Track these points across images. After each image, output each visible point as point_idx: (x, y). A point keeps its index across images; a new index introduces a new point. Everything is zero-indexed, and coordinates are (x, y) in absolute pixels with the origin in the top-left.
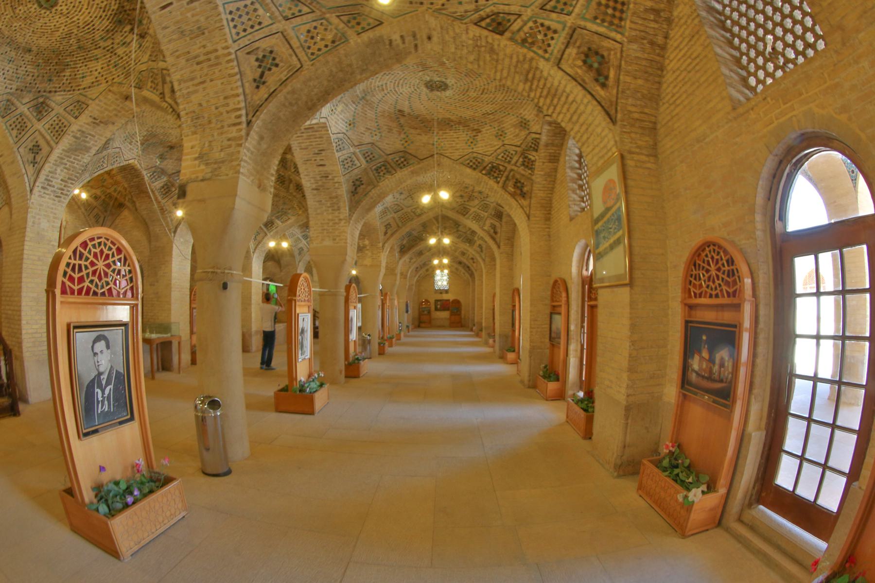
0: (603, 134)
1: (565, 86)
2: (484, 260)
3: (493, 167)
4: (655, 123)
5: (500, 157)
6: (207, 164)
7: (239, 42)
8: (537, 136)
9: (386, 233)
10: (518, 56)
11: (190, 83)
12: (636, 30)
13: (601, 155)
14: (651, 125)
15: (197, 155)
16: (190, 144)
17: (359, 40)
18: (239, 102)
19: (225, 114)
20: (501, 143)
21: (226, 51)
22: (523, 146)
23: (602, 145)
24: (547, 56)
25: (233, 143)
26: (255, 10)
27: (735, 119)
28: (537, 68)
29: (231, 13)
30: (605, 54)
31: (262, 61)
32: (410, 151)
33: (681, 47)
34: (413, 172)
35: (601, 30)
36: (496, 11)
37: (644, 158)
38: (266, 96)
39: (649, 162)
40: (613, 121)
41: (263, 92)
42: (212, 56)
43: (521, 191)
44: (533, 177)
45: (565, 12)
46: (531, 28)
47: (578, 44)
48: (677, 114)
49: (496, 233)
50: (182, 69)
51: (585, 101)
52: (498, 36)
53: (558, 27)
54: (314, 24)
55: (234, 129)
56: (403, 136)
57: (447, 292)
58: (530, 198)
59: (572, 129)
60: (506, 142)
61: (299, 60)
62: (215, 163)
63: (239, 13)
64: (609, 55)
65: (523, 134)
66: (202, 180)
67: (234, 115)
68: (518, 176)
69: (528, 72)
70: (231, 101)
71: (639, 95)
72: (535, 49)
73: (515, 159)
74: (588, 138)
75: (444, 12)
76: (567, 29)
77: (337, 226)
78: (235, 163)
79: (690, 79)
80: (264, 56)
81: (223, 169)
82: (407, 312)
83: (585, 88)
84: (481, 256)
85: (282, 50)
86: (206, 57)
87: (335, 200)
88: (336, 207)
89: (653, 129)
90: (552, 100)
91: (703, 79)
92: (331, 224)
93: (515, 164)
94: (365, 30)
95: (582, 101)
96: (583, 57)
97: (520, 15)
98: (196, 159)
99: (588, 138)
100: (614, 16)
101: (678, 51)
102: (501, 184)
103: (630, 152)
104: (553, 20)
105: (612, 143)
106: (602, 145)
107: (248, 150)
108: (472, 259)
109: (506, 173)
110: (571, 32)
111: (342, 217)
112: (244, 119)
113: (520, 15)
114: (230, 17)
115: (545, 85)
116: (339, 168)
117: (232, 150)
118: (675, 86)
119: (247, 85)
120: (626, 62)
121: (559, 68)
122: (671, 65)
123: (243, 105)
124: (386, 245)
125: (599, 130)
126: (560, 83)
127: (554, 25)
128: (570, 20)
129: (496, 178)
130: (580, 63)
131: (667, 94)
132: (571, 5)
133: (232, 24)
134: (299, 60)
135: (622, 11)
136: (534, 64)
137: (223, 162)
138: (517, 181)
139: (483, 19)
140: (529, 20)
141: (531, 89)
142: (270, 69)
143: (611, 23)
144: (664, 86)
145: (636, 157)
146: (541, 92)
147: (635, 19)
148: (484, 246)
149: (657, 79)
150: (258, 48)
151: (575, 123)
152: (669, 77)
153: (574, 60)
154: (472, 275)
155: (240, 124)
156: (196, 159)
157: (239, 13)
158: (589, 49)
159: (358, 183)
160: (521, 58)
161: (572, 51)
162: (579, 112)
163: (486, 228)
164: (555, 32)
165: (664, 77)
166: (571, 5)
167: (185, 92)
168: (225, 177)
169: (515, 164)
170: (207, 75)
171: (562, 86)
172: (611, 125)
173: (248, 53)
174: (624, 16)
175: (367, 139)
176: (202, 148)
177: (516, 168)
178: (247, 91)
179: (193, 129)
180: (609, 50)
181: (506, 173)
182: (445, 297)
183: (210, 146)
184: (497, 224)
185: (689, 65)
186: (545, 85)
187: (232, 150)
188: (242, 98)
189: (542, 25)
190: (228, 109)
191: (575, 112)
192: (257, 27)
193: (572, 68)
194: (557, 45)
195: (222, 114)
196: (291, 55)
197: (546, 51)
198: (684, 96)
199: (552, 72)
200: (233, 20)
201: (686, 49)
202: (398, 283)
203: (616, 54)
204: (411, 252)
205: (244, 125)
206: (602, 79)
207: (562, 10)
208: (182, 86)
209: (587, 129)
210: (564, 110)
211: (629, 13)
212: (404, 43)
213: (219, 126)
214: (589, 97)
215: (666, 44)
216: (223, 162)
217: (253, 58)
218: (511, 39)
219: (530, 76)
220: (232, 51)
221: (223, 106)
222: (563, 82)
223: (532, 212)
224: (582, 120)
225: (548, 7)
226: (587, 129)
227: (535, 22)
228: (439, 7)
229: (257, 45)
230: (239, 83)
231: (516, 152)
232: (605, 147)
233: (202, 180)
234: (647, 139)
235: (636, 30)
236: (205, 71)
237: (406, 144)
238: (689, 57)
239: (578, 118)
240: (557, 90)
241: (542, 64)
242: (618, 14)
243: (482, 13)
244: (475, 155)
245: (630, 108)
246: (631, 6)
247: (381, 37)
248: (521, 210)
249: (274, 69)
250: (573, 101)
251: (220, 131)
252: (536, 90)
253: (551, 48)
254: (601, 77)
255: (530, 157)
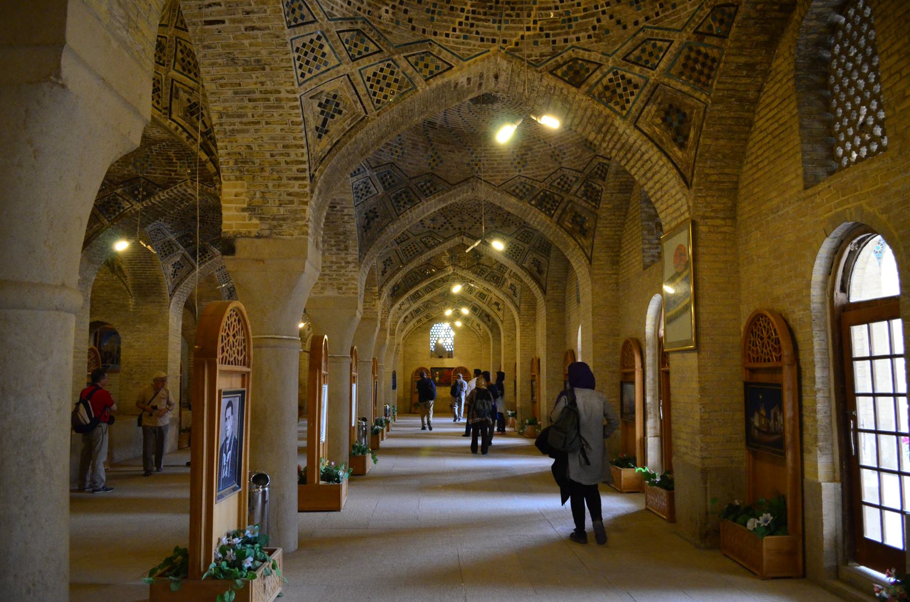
0: (678, 197)
1: (641, 146)
2: (517, 307)
3: (546, 195)
4: (737, 183)
5: (555, 184)
6: (261, 219)
7: (305, 85)
8: (605, 161)
9: (384, 272)
10: (593, 111)
11: (236, 120)
12: (723, 90)
13: (674, 215)
14: (731, 185)
15: (245, 206)
16: (234, 191)
17: (428, 88)
18: (303, 155)
19: (283, 165)
20: (557, 166)
21: (291, 96)
22: (587, 172)
23: (676, 207)
24: (624, 112)
25: (296, 199)
26: (321, 46)
27: (804, 199)
28: (612, 125)
29: (297, 50)
30: (688, 112)
31: (325, 107)
32: (437, 173)
33: (773, 106)
34: (439, 201)
35: (686, 89)
36: (574, 56)
37: (720, 222)
38: (329, 147)
39: (725, 225)
40: (688, 185)
41: (325, 144)
42: (272, 97)
43: (582, 227)
44: (598, 212)
45: (649, 65)
46: (611, 80)
47: (659, 100)
48: (757, 178)
49: (540, 272)
50: (225, 101)
51: (661, 163)
52: (574, 89)
53: (641, 82)
54: (381, 65)
55: (297, 183)
56: (430, 153)
57: (450, 355)
58: (594, 237)
59: (645, 184)
60: (564, 165)
61: (364, 108)
62: (274, 219)
63: (305, 50)
64: (692, 113)
65: (587, 155)
66: (257, 237)
67: (295, 168)
68: (578, 209)
69: (602, 126)
70: (292, 152)
71: (720, 156)
72: (612, 104)
73: (575, 188)
74: (662, 196)
75: (517, 54)
76: (648, 85)
77: (343, 271)
78: (300, 223)
79: (773, 145)
80: (327, 101)
81: (285, 227)
82: (394, 387)
83: (661, 150)
84: (513, 302)
85: (347, 95)
86: (263, 96)
87: (342, 237)
88: (343, 246)
89: (734, 190)
90: (626, 154)
91: (784, 150)
92: (334, 268)
93: (575, 194)
94: (433, 75)
95: (657, 162)
96: (662, 114)
97: (600, 65)
98: (244, 210)
99: (662, 196)
100: (701, 73)
101: (767, 110)
102: (555, 219)
103: (704, 217)
104: (634, 74)
105: (685, 208)
106: (676, 207)
107: (311, 206)
108: (497, 304)
109: (563, 205)
110: (652, 89)
111: (350, 259)
112: (307, 174)
113: (600, 65)
114: (296, 55)
115: (619, 139)
116: (350, 197)
117: (294, 206)
118: (760, 148)
119: (310, 134)
120: (708, 124)
121: (636, 127)
122: (760, 123)
123: (305, 158)
124: (384, 289)
125: (673, 192)
126: (635, 142)
127: (635, 79)
128: (653, 76)
129: (549, 210)
130: (658, 121)
131: (752, 154)
132: (657, 58)
133: (298, 64)
134: (364, 108)
135: (711, 69)
136: (610, 121)
137: (284, 219)
138: (577, 215)
139: (559, 66)
140: (608, 72)
141: (603, 140)
142: (333, 117)
143: (698, 81)
144: (751, 144)
145: (710, 222)
146: (615, 145)
147: (723, 79)
148: (518, 287)
149: (743, 136)
150: (322, 92)
151: (649, 180)
152: (756, 136)
153: (653, 117)
154: (494, 328)
155: (304, 179)
156: (244, 210)
157: (305, 50)
158: (671, 106)
159: (371, 215)
160: (596, 113)
161: (652, 108)
162: (653, 170)
163: (525, 265)
164: (636, 87)
165: (751, 133)
166: (657, 58)
167: (228, 128)
168: (289, 237)
169: (575, 194)
170: (262, 115)
171: (637, 145)
172: (686, 190)
173: (312, 98)
174: (713, 74)
175: (386, 158)
176: (253, 198)
177: (576, 199)
178: (310, 141)
179: (238, 174)
180: (692, 108)
181: (563, 205)
182: (448, 363)
183: (263, 197)
184: (543, 260)
185: (775, 129)
186: (619, 139)
187: (294, 206)
188: (305, 150)
189: (623, 77)
190: (288, 159)
191: (650, 169)
192: (323, 68)
193: (650, 126)
194: (635, 102)
195: (280, 163)
196: (355, 102)
197: (623, 108)
198: (766, 162)
199: (628, 131)
200: (299, 58)
201: (776, 111)
202: (387, 342)
203: (698, 113)
204: (406, 296)
205: (307, 182)
206: (681, 140)
207: (647, 62)
208: (223, 120)
209: (662, 188)
210: (639, 165)
211: (718, 73)
212: (469, 83)
213: (275, 176)
214: (664, 159)
215: (759, 97)
216: (284, 219)
217: (316, 103)
218: (588, 93)
219: (604, 129)
220: (298, 96)
221: (282, 154)
222: (639, 142)
223: (595, 254)
224: (656, 178)
225: (632, 57)
226: (662, 188)
227: (615, 74)
228: (513, 46)
229: (322, 88)
230: (304, 133)
231: (577, 178)
232: (678, 209)
233: (257, 237)
234: (725, 200)
235: (723, 90)
236: (260, 111)
237: (433, 164)
238: (777, 121)
239: (653, 176)
240: (631, 147)
241: (618, 122)
242: (706, 71)
243: (559, 58)
244: (523, 179)
245: (707, 171)
246: (722, 65)
247: (449, 82)
248: (581, 252)
249: (337, 116)
250: (647, 161)
251: (276, 183)
252: (609, 142)
253: (630, 104)
254: (680, 139)
255: (594, 185)
